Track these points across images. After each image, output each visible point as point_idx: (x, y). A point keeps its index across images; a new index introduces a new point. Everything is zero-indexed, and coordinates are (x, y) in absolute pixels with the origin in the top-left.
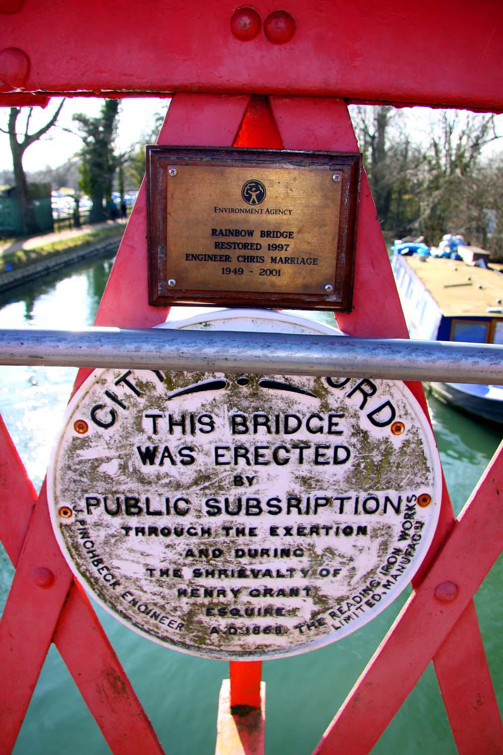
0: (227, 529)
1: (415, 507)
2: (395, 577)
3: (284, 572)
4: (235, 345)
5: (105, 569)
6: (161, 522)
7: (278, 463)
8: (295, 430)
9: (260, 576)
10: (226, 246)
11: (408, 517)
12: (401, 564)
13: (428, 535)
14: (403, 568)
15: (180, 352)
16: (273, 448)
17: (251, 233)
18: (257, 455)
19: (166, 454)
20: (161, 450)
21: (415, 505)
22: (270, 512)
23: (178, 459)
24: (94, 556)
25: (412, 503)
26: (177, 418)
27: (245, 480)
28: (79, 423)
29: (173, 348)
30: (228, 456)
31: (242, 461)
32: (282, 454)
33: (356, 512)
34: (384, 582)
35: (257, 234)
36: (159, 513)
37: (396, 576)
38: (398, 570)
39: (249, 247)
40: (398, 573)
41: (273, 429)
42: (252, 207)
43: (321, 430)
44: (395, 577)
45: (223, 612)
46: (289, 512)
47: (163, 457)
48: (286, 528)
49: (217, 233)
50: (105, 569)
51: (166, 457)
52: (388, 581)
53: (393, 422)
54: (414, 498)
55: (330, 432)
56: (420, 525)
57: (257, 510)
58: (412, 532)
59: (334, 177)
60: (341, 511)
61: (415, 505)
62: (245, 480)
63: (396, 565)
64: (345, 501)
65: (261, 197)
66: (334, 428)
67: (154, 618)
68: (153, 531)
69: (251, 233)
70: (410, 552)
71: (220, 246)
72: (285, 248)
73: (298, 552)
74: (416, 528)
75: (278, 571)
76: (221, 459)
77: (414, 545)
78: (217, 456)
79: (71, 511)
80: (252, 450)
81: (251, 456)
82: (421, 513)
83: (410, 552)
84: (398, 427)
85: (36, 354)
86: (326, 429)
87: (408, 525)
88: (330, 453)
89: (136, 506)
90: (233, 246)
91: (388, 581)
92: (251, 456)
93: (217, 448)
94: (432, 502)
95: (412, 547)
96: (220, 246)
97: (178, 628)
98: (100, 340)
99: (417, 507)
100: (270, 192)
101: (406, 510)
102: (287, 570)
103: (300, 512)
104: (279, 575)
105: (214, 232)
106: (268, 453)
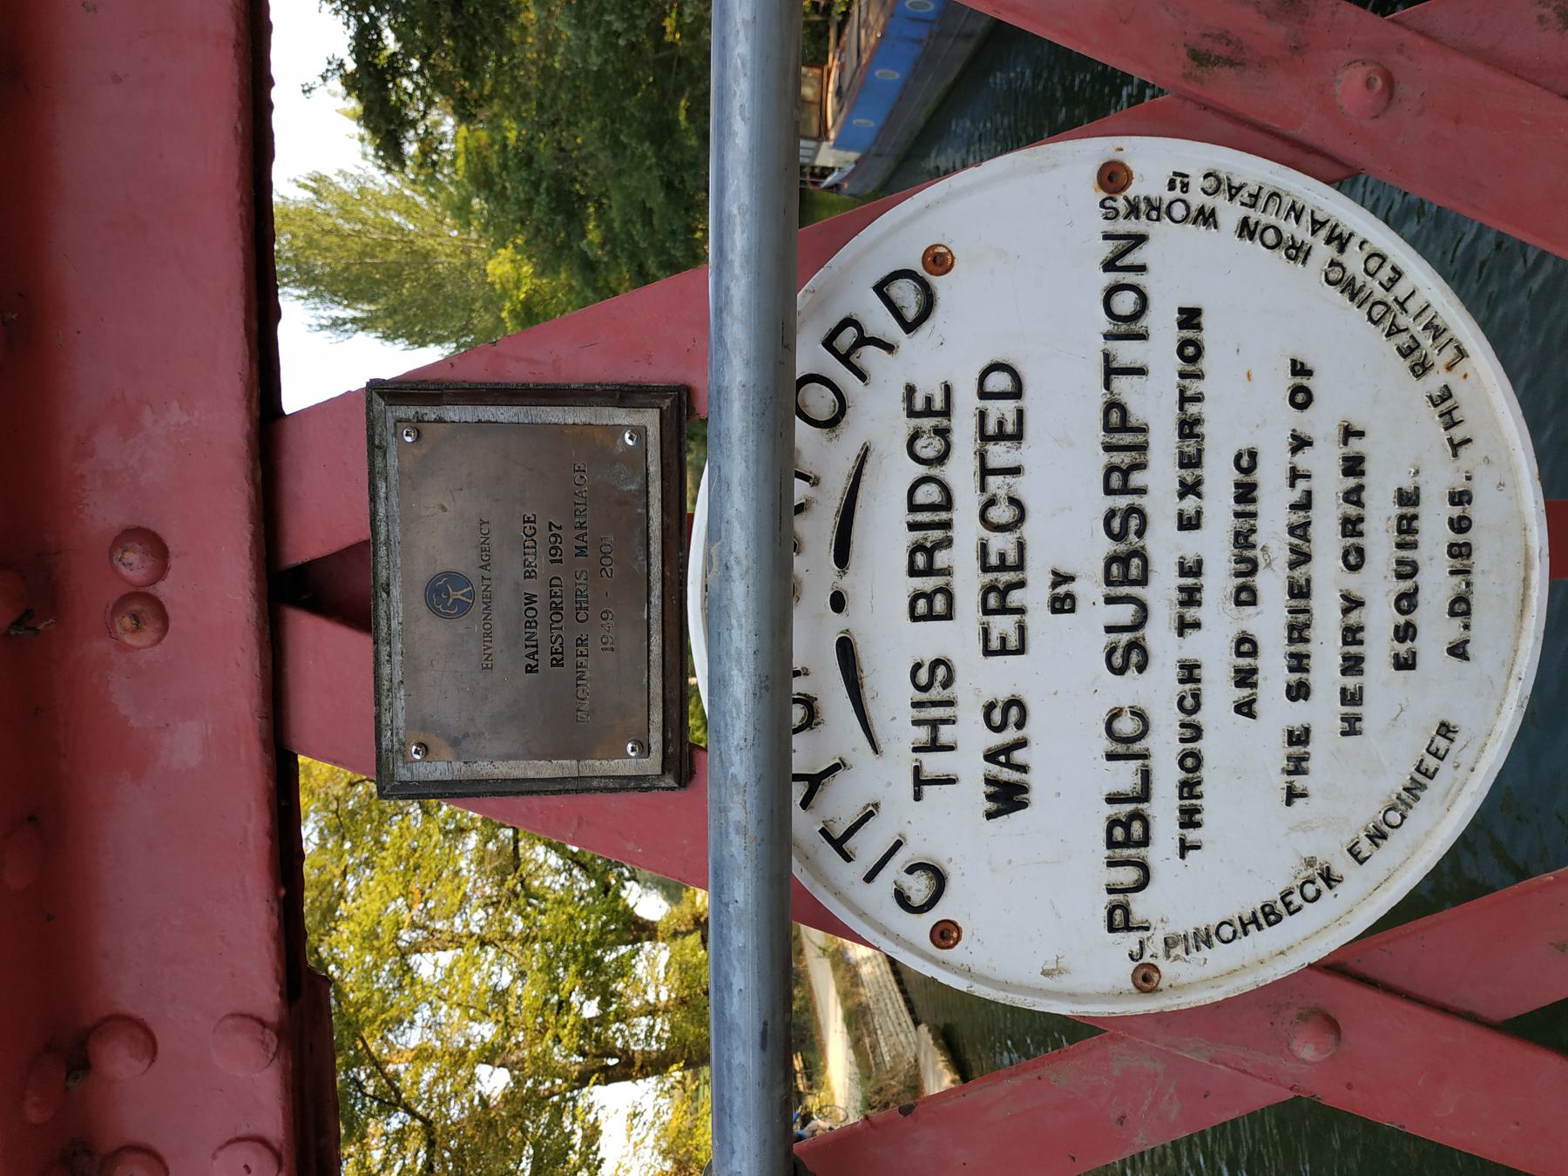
0: (1185, 626)
1: (1131, 198)
2: (1317, 225)
3: (1296, 495)
4: (725, 635)
5: (1288, 899)
6: (1167, 777)
7: (1021, 517)
8: (945, 489)
9: (1304, 547)
10: (556, 646)
11: (1155, 209)
12: (1283, 213)
13: (1197, 157)
14: (1293, 207)
15: (742, 743)
16: (986, 533)
17: (530, 599)
18: (1003, 566)
19: (1002, 759)
20: (995, 769)
21: (1126, 199)
22: (1140, 533)
23: (1010, 735)
24: (1254, 920)
25: (1121, 204)
26: (923, 734)
27: (1062, 590)
28: (937, 937)
29: (736, 758)
30: (1003, 625)
31: (1015, 598)
32: (1002, 513)
33: (1142, 337)
34: (1330, 252)
35: (532, 587)
36: (1146, 775)
37: (1314, 221)
38: (1298, 219)
39: (558, 600)
40: (1306, 218)
41: (937, 534)
42: (479, 599)
43: (943, 433)
44: (1317, 225)
45: (1406, 631)
46: (1141, 491)
47: (1009, 765)
48: (1182, 496)
49: (533, 663)
50: (1288, 899)
51: (1008, 759)
52: (1328, 241)
53: (922, 272)
54: (1108, 203)
55: (946, 413)
56: (1179, 181)
57: (1136, 562)
58: (1196, 198)
59: (409, 439)
60: (1140, 371)
61: (1126, 199)
62: (1062, 590)
63: (1281, 224)
64: (1115, 365)
65: (455, 578)
66: (938, 404)
67: (1418, 792)
68: (1189, 788)
69: (530, 599)
70: (1250, 195)
71: (558, 657)
72: (555, 531)
73: (1245, 462)
74: (1185, 187)
75: (1294, 507)
76: (1013, 643)
77: (1230, 187)
78: (1004, 651)
79: (1144, 965)
80: (990, 576)
81: (1006, 577)
82: (1148, 181)
83: (1250, 195)
84: (934, 260)
85: (757, 1037)
86: (941, 422)
87: (1179, 210)
88: (997, 409)
89: (1127, 827)
90: (556, 633)
91: (1328, 241)
92: (1006, 577)
93: (987, 652)
94: (1118, 156)
95: (1234, 191)
96: (558, 657)
97: (1451, 735)
98: (727, 905)
99: (1131, 192)
100: (448, 561)
101: (1137, 218)
102: (1292, 485)
103: (1141, 466)
104: (1305, 504)
105: (530, 669)
106: (1001, 543)
